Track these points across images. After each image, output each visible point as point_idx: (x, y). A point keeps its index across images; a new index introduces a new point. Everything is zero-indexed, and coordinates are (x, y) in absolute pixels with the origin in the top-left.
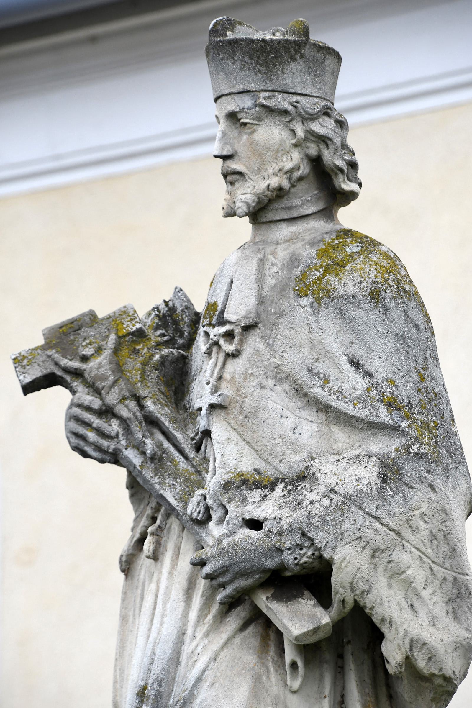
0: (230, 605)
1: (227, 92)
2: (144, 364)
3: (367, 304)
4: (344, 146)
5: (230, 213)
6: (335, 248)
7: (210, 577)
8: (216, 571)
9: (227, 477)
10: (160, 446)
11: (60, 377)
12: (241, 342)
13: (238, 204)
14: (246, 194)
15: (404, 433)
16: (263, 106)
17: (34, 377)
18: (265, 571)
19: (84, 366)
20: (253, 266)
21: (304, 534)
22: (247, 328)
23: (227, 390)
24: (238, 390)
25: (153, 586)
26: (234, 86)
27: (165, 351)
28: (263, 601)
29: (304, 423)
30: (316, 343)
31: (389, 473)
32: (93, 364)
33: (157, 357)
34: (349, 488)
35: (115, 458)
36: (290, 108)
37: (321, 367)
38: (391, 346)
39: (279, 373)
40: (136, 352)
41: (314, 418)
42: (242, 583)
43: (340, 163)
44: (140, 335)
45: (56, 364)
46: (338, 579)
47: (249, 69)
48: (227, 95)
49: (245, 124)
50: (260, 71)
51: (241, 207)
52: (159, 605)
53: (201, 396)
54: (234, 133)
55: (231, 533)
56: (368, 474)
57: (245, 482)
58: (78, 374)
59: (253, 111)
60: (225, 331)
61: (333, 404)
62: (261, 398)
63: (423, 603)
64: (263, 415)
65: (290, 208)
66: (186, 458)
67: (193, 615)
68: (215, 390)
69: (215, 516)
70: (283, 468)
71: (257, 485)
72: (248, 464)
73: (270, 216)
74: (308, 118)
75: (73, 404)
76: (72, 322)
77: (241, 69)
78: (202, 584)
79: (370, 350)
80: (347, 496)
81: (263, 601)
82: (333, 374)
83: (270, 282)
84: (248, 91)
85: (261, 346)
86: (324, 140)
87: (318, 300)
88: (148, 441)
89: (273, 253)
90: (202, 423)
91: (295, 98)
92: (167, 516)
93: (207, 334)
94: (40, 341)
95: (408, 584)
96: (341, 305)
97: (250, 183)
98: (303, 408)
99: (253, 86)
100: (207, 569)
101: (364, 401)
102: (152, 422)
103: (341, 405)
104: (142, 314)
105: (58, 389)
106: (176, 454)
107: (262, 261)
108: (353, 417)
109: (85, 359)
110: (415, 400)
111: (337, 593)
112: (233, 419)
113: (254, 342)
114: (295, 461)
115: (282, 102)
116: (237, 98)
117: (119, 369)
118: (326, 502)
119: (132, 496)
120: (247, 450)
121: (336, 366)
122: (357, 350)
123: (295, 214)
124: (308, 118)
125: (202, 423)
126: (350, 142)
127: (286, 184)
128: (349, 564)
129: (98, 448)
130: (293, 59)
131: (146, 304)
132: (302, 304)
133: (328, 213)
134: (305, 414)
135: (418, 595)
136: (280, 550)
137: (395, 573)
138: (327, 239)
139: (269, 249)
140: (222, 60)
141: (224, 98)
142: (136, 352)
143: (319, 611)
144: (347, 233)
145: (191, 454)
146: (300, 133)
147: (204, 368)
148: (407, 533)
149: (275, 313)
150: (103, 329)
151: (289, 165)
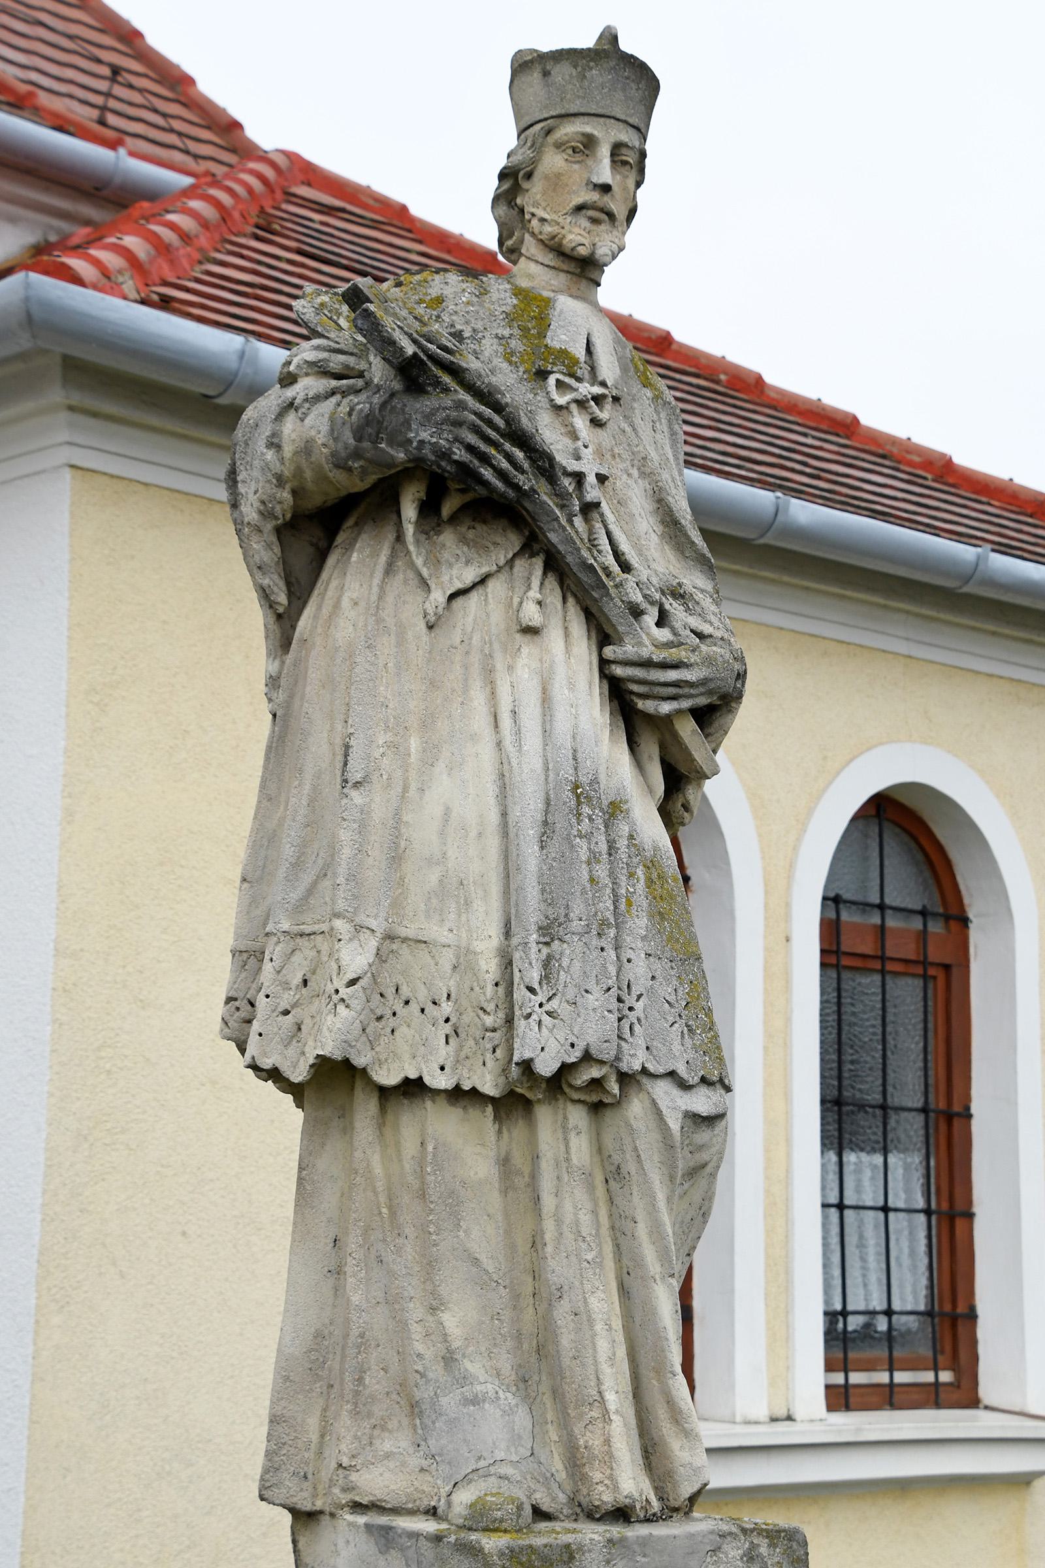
1: (623, 117)
26: (631, 116)
29: (651, 530)
48: (618, 120)
108: (693, 542)
116: (631, 131)
140: (627, 78)
141: (612, 121)
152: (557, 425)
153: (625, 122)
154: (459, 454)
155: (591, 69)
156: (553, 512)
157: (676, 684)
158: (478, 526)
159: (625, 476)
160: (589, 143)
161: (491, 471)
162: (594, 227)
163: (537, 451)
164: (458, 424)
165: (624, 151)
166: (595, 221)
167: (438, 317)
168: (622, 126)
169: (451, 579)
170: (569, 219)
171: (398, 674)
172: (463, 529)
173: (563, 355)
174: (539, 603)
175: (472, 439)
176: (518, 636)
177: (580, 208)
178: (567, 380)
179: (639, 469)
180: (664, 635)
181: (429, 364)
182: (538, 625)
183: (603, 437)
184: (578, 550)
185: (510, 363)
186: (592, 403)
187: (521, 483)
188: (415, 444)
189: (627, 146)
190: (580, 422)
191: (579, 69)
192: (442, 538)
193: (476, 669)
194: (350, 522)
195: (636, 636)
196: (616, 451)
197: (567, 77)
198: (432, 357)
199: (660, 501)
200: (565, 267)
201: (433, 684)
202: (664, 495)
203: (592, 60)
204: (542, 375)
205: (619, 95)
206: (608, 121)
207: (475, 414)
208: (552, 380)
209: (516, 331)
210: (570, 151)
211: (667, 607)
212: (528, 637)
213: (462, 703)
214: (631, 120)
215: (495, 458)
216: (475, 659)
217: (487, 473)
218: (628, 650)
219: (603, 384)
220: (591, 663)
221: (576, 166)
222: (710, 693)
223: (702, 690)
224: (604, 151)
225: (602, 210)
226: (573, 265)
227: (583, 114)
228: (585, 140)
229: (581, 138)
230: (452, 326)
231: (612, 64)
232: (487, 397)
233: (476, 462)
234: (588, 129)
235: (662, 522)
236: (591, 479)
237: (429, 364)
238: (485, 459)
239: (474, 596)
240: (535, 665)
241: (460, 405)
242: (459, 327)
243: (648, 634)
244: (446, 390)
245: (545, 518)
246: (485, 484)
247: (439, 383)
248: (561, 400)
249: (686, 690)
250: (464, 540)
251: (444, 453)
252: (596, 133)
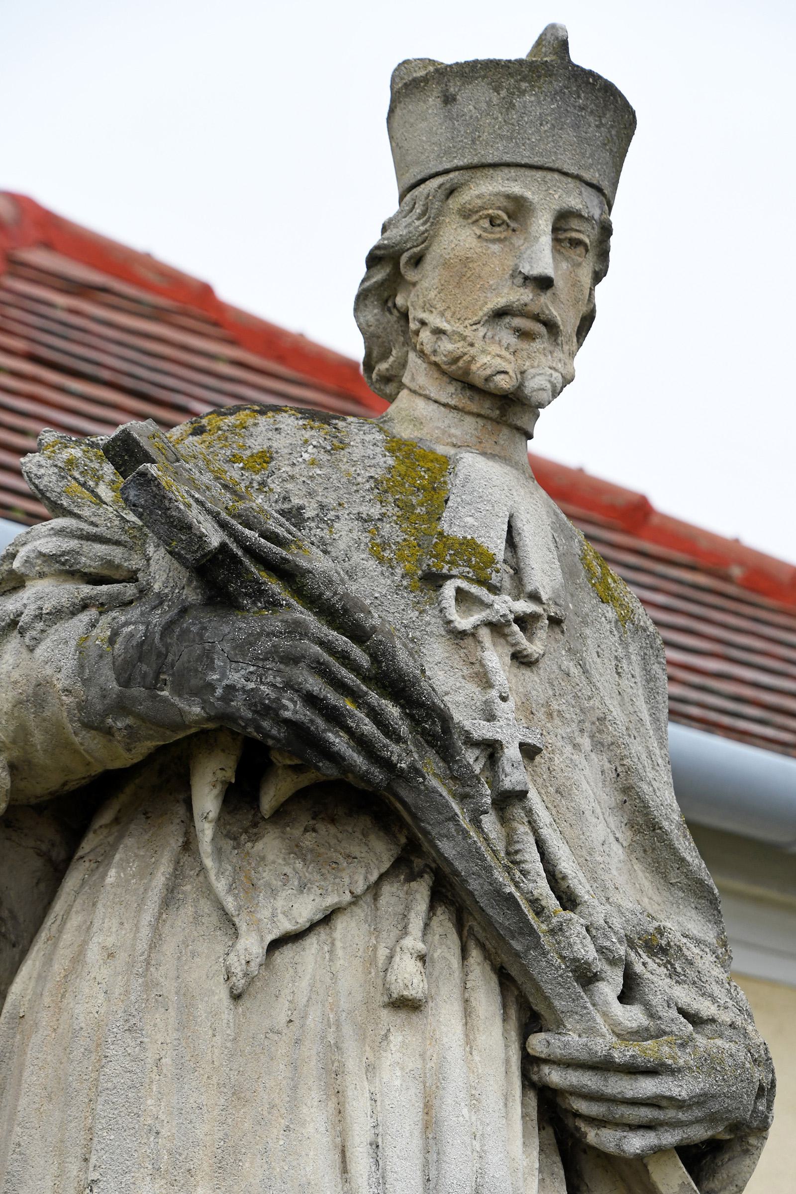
1: (573, 170)
26: (588, 168)
39: (600, 731)
48: (566, 174)
49: (576, 243)
60: (529, 611)
108: (683, 860)
116: (587, 192)
140: (582, 108)
141: (556, 176)
152: (457, 662)
153: (578, 178)
154: (293, 709)
155: (523, 93)
156: (447, 806)
157: (653, 1102)
158: (321, 827)
159: (569, 749)
160: (517, 211)
161: (346, 737)
162: (524, 345)
163: (422, 705)
164: (292, 659)
165: (574, 223)
166: (524, 335)
167: (263, 484)
168: (571, 183)
169: (274, 915)
170: (482, 331)
171: (179, 1077)
172: (297, 832)
173: (469, 550)
174: (422, 958)
175: (314, 684)
176: (385, 1013)
177: (500, 314)
178: (475, 589)
179: (592, 737)
180: (632, 1016)
181: (247, 561)
182: (420, 995)
183: (532, 682)
184: (489, 869)
185: (381, 560)
186: (516, 628)
187: (395, 758)
188: (219, 692)
189: (578, 215)
190: (495, 658)
191: (503, 93)
192: (259, 845)
193: (312, 1069)
194: (106, 817)
195: (585, 1017)
196: (555, 706)
197: (484, 106)
198: (251, 551)
199: (627, 790)
200: (474, 408)
201: (238, 1095)
202: (634, 780)
203: (524, 79)
204: (433, 580)
205: (569, 135)
206: (549, 175)
207: (321, 643)
208: (449, 589)
209: (392, 510)
210: (486, 223)
211: (638, 968)
212: (402, 1015)
213: (287, 1129)
214: (587, 176)
215: (352, 716)
216: (311, 1050)
217: (338, 741)
218: (571, 1040)
219: (535, 597)
220: (507, 1061)
221: (495, 248)
222: (712, 1119)
223: (698, 1113)
224: (543, 224)
225: (536, 318)
226: (487, 404)
227: (508, 165)
228: (510, 206)
229: (504, 203)
230: (286, 499)
231: (557, 85)
232: (340, 615)
233: (321, 723)
234: (516, 189)
235: (631, 824)
236: (512, 752)
237: (247, 561)
238: (335, 717)
239: (312, 945)
240: (414, 1063)
241: (296, 629)
242: (296, 501)
243: (605, 1015)
244: (274, 604)
245: (433, 816)
246: (335, 758)
247: (262, 592)
248: (464, 623)
249: (671, 1114)
250: (296, 850)
251: (267, 708)
252: (528, 194)
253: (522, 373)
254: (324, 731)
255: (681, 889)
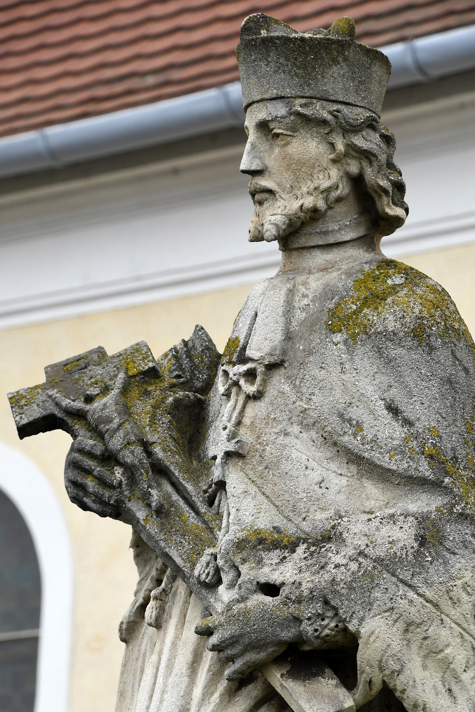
0: (240, 682)
1: (259, 98)
2: (155, 407)
3: (409, 343)
4: (390, 165)
5: (258, 237)
6: (375, 279)
7: (214, 648)
8: (224, 641)
9: (241, 535)
10: (168, 497)
11: (60, 419)
12: (265, 382)
13: (267, 226)
14: (275, 215)
15: (447, 490)
16: (298, 114)
17: (32, 419)
18: (280, 643)
19: (88, 407)
20: (280, 297)
21: (326, 602)
22: (272, 367)
23: (245, 434)
24: (258, 437)
25: (154, 658)
26: (266, 92)
27: (180, 394)
28: (278, 679)
29: (333, 476)
30: (349, 385)
31: (429, 536)
32: (97, 405)
33: (171, 399)
34: (381, 552)
35: (116, 511)
36: (329, 117)
37: (355, 413)
38: (435, 390)
40: (147, 393)
41: (344, 471)
42: (252, 657)
43: (384, 183)
44: (153, 374)
45: (57, 404)
46: (366, 656)
47: (284, 72)
48: (258, 102)
49: (277, 135)
50: (296, 75)
51: (270, 230)
52: (160, 680)
53: (217, 444)
54: (263, 146)
55: (243, 599)
56: (404, 535)
57: (261, 541)
58: (80, 415)
59: (287, 120)
61: (366, 455)
62: (285, 446)
63: (464, 688)
64: (285, 466)
65: (326, 233)
66: (197, 513)
67: (198, 692)
68: (232, 436)
69: (226, 578)
70: (306, 526)
71: (276, 545)
72: (265, 520)
73: (303, 241)
74: (350, 129)
75: (73, 449)
76: (79, 359)
77: (275, 72)
78: (209, 657)
79: (410, 394)
80: (378, 560)
81: (278, 679)
82: (367, 420)
83: (300, 315)
84: (282, 98)
85: (287, 388)
86: (367, 155)
87: (354, 336)
88: (154, 492)
89: (305, 284)
90: (216, 473)
91: (335, 107)
92: (174, 578)
93: (226, 373)
94: (42, 379)
95: (446, 665)
96: (380, 342)
97: (280, 203)
98: (331, 459)
99: (288, 92)
100: (214, 640)
101: (402, 452)
102: (160, 471)
103: (376, 456)
104: (157, 354)
105: (59, 433)
106: (185, 508)
107: (291, 292)
108: (389, 470)
109: (89, 399)
110: (461, 452)
111: (363, 672)
112: (252, 469)
113: (279, 383)
114: (320, 518)
115: (321, 110)
117: (126, 411)
118: (354, 566)
119: (137, 556)
120: (266, 504)
121: (372, 412)
122: (396, 394)
123: (331, 240)
124: (350, 129)
125: (216, 473)
126: (397, 161)
127: (321, 204)
128: (377, 636)
129: (99, 499)
130: (335, 62)
131: (163, 342)
132: (335, 340)
133: (369, 241)
134: (333, 466)
135: (457, 679)
136: (297, 620)
137: (432, 652)
138: (366, 268)
139: (300, 279)
141: (255, 105)
142: (147, 393)
143: (342, 692)
144: (390, 264)
145: (203, 509)
146: (340, 147)
147: (223, 412)
148: (446, 605)
149: (304, 350)
150: (111, 368)
151: (325, 184)
199: (335, 444)
202: (335, 438)
253: (263, 225)
254: (83, 497)
255: (405, 485)
